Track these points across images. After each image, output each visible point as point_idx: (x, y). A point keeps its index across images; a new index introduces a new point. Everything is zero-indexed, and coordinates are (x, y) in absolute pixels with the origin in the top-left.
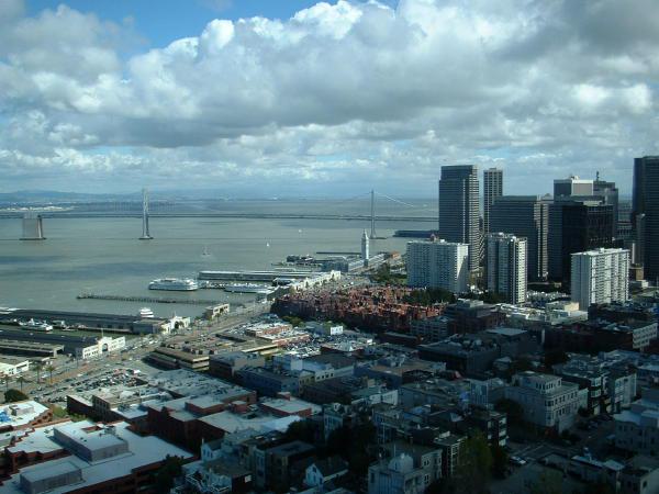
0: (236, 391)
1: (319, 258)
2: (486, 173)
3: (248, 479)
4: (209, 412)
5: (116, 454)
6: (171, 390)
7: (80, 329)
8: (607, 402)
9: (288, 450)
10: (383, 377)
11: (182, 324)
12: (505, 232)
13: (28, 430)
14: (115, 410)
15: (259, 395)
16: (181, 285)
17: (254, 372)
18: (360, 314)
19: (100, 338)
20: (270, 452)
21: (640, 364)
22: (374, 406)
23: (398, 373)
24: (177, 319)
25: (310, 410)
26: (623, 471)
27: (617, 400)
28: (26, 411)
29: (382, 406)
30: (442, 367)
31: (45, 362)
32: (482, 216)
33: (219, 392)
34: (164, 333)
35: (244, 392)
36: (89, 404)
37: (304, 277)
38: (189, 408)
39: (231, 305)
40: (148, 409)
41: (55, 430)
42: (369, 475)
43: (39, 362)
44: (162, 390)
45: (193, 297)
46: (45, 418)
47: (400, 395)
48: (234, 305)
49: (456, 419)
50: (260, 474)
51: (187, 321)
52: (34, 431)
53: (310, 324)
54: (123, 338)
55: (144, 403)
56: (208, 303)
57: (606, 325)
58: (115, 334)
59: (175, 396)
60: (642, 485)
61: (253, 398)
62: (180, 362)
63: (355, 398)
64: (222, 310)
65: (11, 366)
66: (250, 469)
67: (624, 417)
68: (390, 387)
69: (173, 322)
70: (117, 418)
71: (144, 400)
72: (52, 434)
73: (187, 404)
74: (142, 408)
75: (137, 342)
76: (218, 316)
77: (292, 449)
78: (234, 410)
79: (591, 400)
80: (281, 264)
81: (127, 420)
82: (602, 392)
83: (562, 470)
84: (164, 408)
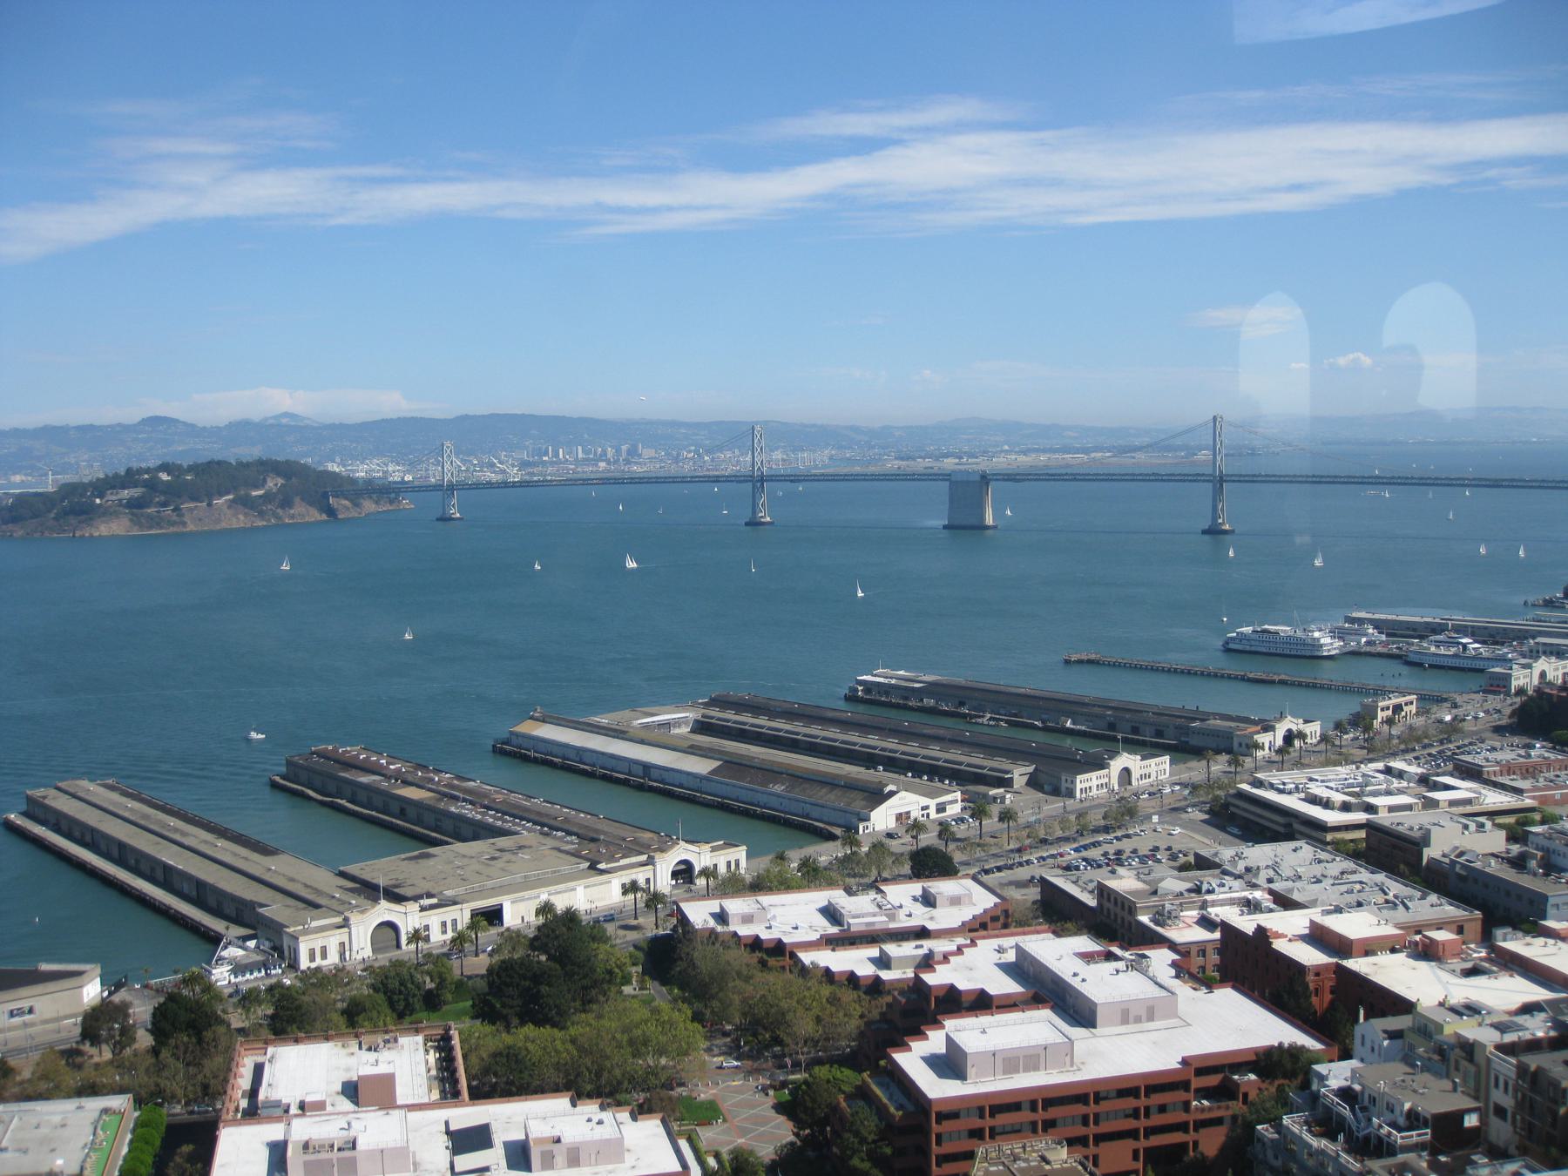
0: (1431, 907)
4: (1369, 948)
5: (1151, 1018)
6: (1276, 886)
7: (1070, 732)
11: (1302, 736)
13: (960, 941)
14: (1144, 919)
16: (1302, 643)
17: (1478, 865)
19: (1114, 754)
24: (1289, 724)
28: (955, 901)
31: (995, 799)
33: (1391, 904)
34: (1260, 754)
35: (1450, 911)
36: (1091, 901)
38: (1319, 937)
39: (1422, 698)
40: (1226, 928)
41: (1018, 948)
43: (985, 796)
44: (1254, 886)
45: (1327, 673)
46: (994, 919)
48: (1428, 701)
50: (1500, 1112)
51: (1314, 730)
52: (973, 943)
54: (1167, 758)
55: (1215, 912)
56: (1362, 691)
58: (1147, 747)
59: (1285, 902)
61: (1474, 928)
62: (1297, 826)
64: (1398, 708)
65: (925, 801)
69: (1281, 729)
70: (1160, 941)
71: (1214, 904)
72: (1011, 956)
73: (1314, 926)
74: (1206, 923)
75: (1196, 771)
76: (1389, 722)
78: (1427, 952)
80: (1549, 604)
81: (1173, 946)
84: (1261, 931)
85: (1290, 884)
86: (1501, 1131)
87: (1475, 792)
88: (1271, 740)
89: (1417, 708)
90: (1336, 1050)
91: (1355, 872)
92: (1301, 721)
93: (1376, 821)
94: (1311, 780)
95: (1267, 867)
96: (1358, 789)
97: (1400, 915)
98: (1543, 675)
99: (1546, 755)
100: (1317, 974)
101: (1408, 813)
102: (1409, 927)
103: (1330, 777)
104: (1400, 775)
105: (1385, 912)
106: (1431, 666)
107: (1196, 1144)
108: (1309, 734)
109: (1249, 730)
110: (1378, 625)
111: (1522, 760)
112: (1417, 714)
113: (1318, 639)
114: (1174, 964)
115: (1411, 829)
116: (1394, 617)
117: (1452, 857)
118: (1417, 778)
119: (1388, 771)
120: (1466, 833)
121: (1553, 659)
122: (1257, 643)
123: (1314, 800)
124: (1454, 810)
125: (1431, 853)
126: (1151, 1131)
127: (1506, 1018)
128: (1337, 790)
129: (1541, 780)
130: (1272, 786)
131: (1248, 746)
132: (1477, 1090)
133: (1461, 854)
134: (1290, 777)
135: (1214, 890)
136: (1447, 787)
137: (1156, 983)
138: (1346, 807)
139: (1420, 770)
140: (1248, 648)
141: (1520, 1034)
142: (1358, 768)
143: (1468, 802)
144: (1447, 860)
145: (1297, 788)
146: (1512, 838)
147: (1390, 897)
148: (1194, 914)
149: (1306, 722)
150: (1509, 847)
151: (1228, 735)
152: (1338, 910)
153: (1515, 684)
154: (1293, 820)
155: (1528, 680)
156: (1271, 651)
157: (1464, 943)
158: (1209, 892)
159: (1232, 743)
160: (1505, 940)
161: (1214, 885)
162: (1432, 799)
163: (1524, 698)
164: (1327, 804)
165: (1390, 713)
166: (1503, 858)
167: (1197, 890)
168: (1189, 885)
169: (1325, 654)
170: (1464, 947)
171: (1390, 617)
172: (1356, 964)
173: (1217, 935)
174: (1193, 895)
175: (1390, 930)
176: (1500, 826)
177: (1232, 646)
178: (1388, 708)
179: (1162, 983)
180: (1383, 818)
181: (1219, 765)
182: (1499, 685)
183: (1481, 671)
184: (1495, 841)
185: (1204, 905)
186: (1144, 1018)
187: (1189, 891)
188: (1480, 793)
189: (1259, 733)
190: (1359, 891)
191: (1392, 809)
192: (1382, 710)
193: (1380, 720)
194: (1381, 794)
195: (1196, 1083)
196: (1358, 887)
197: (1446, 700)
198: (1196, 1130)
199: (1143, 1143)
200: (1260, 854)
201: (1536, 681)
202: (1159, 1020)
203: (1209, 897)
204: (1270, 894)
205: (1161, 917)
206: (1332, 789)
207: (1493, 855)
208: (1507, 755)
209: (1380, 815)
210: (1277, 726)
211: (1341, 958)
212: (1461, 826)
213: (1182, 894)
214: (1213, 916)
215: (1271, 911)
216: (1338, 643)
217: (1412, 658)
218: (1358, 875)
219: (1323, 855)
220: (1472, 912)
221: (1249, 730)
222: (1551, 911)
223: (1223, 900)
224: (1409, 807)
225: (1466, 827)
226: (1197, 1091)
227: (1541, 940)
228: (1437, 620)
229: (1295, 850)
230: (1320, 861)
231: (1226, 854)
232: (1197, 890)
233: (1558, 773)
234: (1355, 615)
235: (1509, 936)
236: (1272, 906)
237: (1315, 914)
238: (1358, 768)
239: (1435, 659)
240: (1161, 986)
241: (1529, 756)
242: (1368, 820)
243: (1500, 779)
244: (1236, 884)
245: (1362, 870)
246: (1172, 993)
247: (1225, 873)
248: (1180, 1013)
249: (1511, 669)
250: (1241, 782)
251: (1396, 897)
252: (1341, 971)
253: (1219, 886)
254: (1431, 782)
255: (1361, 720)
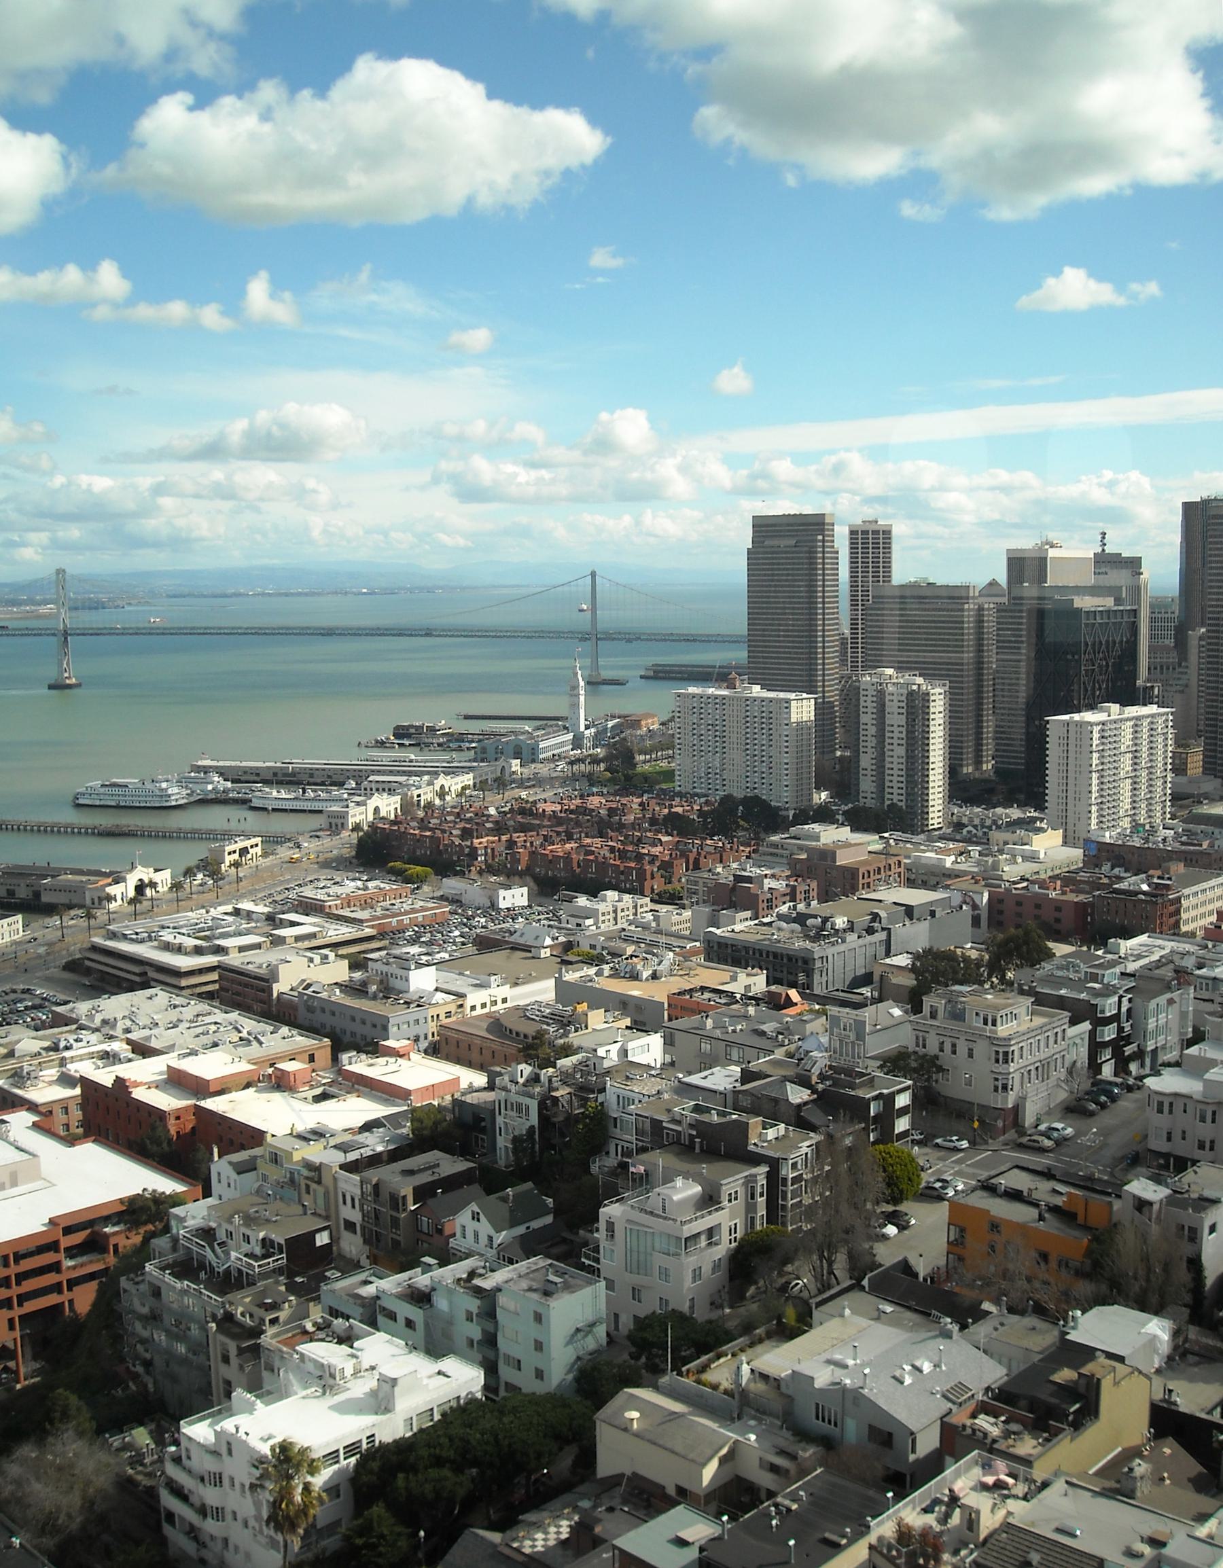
1: (475, 727)
2: (853, 533)
3: (322, 1239)
5: (14, 1183)
6: (133, 1036)
8: (1128, 1050)
9: (410, 1173)
10: (623, 1004)
11: (153, 885)
12: (899, 669)
15: (338, 1048)
17: (324, 995)
18: (567, 858)
20: (374, 1175)
21: (1200, 966)
22: (608, 1072)
23: (659, 993)
24: (142, 873)
25: (457, 1080)
26: (1170, 1201)
27: (1150, 1046)
29: (628, 1069)
30: (758, 982)
32: (847, 631)
34: (113, 906)
35: (301, 1041)
37: (436, 774)
38: (177, 1081)
40: (85, 1082)
42: (602, 1225)
47: (669, 1042)
48: (272, 842)
49: (797, 1095)
50: (350, 1226)
51: (164, 878)
53: (452, 885)
54: (19, 917)
55: (75, 1069)
57: (1120, 879)
59: (142, 1050)
60: (1206, 1231)
61: (324, 1056)
62: (152, 974)
63: (567, 1051)
64: (244, 851)
66: (327, 1218)
67: (1167, 1083)
68: (640, 1027)
69: (132, 880)
74: (66, 1080)
76: (236, 865)
77: (420, 1171)
78: (281, 1083)
79: (1095, 1047)
80: (381, 744)
81: (32, 1107)
82: (1120, 1029)
83: (1035, 1205)
84: (119, 1081)
85: (146, 1032)
86: (352, 1245)
87: (318, 926)
88: (122, 891)
89: (263, 849)
90: (199, 1189)
91: (210, 1014)
92: (151, 870)
93: (227, 962)
94: (163, 927)
95: (124, 1017)
96: (207, 933)
97: (254, 1050)
98: (377, 810)
99: (382, 885)
100: (178, 1118)
101: (258, 951)
102: (263, 1061)
103: (181, 923)
104: (249, 915)
105: (240, 1049)
106: (273, 810)
107: (71, 1302)
108: (159, 882)
109: (101, 883)
110: (222, 772)
111: (361, 892)
112: (265, 855)
113: (166, 790)
114: (36, 1126)
115: (260, 967)
116: (238, 763)
117: (300, 990)
118: (264, 917)
119: (237, 912)
120: (311, 965)
121: (385, 795)
122: (107, 797)
123: (167, 947)
124: (300, 944)
125: (281, 987)
126: (22, 1299)
127: (347, 1137)
128: (189, 936)
129: (379, 909)
130: (125, 937)
131: (100, 899)
132: (327, 1209)
133: (309, 986)
134: (141, 926)
135: (71, 1045)
136: (293, 924)
137: (17, 1148)
138: (198, 951)
139: (266, 910)
140: (98, 803)
141: (362, 1151)
142: (207, 912)
143: (313, 936)
144: (296, 994)
145: (150, 937)
146: (354, 966)
147: (244, 1034)
148: (52, 1073)
149: (156, 871)
150: (353, 975)
151: (78, 889)
152: (193, 1053)
153: (351, 821)
154: (147, 968)
155: (364, 816)
156: (134, 804)
157: (314, 1071)
158: (67, 1048)
159: (85, 898)
160: (350, 1064)
161: (72, 1041)
162: (279, 936)
163: (361, 834)
164: (179, 949)
165: (236, 856)
166: (346, 986)
167: (55, 1048)
168: (46, 1044)
169: (174, 803)
170: (314, 1074)
171: (233, 764)
172: (211, 1104)
173: (78, 1091)
174: (51, 1053)
175: (244, 1067)
176: (343, 957)
177: (81, 801)
178: (235, 852)
179: (23, 1146)
180: (234, 959)
181: (73, 921)
182: (336, 824)
183: (320, 812)
184: (339, 971)
185: (63, 1062)
186: (7, 1185)
187: (47, 1049)
188: (323, 927)
189: (110, 885)
190: (214, 1032)
191: (241, 949)
192: (229, 853)
193: (227, 864)
194: (231, 936)
195: (66, 1242)
196: (213, 1028)
197: (290, 840)
198: (70, 1289)
199: (17, 1312)
200: (115, 1006)
201: (370, 818)
202: (26, 1183)
203: (67, 1054)
204: (128, 1044)
205: (19, 1077)
206: (184, 934)
207: (336, 984)
208: (350, 886)
209: (231, 956)
210: (128, 876)
211: (198, 1099)
212: (306, 959)
213: (40, 1054)
214: (72, 1073)
215: (130, 1060)
216: (185, 792)
217: (256, 803)
218: (212, 1016)
219: (178, 1001)
220: (320, 1040)
221: (101, 883)
222: (393, 1030)
223: (81, 1056)
224: (258, 946)
225: (311, 960)
226: (66, 1249)
227: (382, 1060)
228: (279, 765)
229: (150, 998)
230: (175, 1007)
231: (82, 1008)
232: (55, 1048)
233: (394, 902)
234: (200, 763)
235: (354, 1060)
236: (131, 1055)
237: (171, 1059)
238: (207, 912)
239: (277, 802)
240: (22, 1150)
241: (366, 888)
242: (219, 961)
243: (341, 912)
244: (94, 1038)
245: (216, 1011)
246: (34, 1156)
247: (81, 1028)
248: (44, 1173)
249: (347, 807)
250: (96, 935)
251: (249, 1033)
252: (199, 1111)
253: (76, 1041)
254: (278, 921)
255: (211, 867)
